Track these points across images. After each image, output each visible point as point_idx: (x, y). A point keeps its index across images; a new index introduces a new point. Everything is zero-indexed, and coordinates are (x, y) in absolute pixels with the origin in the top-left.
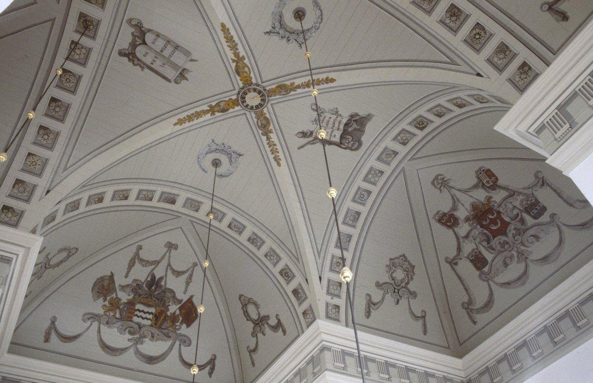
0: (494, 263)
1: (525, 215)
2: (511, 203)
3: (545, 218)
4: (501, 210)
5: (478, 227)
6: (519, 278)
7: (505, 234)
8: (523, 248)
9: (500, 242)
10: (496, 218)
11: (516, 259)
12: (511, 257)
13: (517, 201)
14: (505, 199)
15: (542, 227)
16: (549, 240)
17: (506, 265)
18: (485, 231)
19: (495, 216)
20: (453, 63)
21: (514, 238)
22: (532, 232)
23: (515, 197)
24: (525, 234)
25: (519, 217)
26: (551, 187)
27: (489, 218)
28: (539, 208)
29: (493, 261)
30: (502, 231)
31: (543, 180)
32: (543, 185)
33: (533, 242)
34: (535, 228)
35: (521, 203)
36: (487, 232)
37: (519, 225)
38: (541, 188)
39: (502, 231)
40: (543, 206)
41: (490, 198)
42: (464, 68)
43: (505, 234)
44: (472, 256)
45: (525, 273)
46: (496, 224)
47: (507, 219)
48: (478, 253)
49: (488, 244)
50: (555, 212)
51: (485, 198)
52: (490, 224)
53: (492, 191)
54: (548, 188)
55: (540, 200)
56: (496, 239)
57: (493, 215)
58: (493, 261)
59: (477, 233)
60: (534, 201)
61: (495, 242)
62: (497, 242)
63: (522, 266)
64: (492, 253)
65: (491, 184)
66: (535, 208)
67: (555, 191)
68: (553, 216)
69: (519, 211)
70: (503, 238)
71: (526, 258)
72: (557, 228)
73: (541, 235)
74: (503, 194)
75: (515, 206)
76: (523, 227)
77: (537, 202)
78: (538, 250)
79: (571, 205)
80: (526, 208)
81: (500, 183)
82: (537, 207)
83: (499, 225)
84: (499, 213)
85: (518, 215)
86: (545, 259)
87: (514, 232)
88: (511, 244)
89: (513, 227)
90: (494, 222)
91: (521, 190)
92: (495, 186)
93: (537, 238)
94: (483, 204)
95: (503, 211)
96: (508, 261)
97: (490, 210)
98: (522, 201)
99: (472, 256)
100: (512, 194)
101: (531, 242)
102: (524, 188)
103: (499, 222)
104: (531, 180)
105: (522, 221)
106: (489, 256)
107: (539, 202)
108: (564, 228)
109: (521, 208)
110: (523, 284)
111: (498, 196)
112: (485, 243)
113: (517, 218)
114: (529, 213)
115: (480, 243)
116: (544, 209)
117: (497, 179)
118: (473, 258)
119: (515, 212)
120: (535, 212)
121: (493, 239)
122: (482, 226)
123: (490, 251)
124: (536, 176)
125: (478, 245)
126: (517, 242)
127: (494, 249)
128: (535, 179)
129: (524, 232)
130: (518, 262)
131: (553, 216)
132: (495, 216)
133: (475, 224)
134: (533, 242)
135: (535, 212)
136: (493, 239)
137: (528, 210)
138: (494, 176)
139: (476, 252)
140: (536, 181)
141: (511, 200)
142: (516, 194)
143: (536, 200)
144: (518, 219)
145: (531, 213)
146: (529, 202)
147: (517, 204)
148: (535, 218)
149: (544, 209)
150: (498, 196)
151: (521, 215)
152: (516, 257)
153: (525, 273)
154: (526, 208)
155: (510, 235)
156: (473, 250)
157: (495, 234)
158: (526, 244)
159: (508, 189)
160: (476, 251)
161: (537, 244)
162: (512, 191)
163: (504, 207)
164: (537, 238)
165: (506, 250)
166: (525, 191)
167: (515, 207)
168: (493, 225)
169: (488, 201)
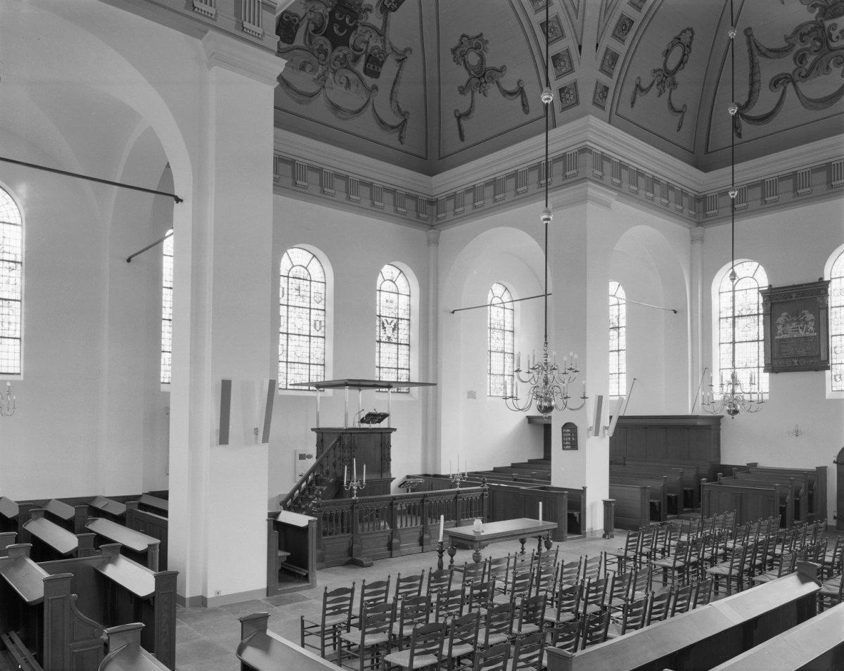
0: (296, 51)
1: (363, 58)
2: (371, 36)
3: (370, 81)
4: (360, 28)
5: (329, 9)
6: (300, 93)
7: (334, 48)
8: (331, 76)
9: (322, 45)
10: (348, 27)
11: (316, 76)
12: (313, 70)
13: (375, 43)
14: (374, 28)
15: (360, 85)
16: (352, 99)
17: (302, 68)
18: (327, 21)
19: (351, 25)
20: (607, 9)
21: (336, 60)
22: (351, 76)
23: (379, 38)
24: (346, 70)
25: (360, 53)
26: (399, 70)
27: (345, 19)
28: (376, 70)
29: (297, 48)
30: (337, 42)
31: (403, 59)
32: (399, 61)
33: (342, 83)
34: (355, 76)
35: (373, 48)
36: (327, 23)
37: (350, 58)
38: (396, 60)
39: (337, 42)
40: (380, 73)
41: (370, 10)
42: (602, 25)
43: (334, 48)
44: (287, 17)
45: (312, 96)
46: (341, 30)
47: (351, 41)
48: (296, 24)
49: (313, 31)
50: (379, 87)
51: (369, 5)
52: (338, 22)
53: (379, 8)
54: (397, 68)
55: (385, 66)
56: (323, 38)
57: (351, 22)
58: (297, 48)
59: (321, 11)
60: (381, 60)
61: (320, 40)
62: (320, 42)
63: (313, 88)
64: (305, 39)
65: (388, 6)
66: (374, 65)
67: (397, 76)
68: (375, 88)
69: (365, 49)
70: (328, 47)
71: (324, 87)
72: (366, 99)
73: (353, 87)
74: (379, 24)
75: (368, 42)
76: (350, 63)
77: (381, 64)
78: (337, 93)
79: (391, 99)
80: (370, 55)
81: (393, 16)
82: (376, 67)
83: (341, 35)
84: (355, 27)
85: (361, 50)
86: (336, 108)
87: (341, 57)
88: (327, 60)
89: (346, 52)
90: (343, 27)
91: (388, 42)
92: (385, 10)
93: (348, 85)
94: (360, 4)
95: (358, 32)
96: (308, 68)
97: (355, 16)
98: (377, 47)
99: (287, 17)
100: (382, 34)
101: (341, 81)
102: (390, 43)
103: (345, 32)
104: (401, 47)
105: (356, 59)
106: (299, 40)
107: (381, 67)
108: (370, 108)
109: (368, 51)
110: (300, 102)
111: (374, 19)
112: (312, 27)
113: (358, 51)
114: (367, 61)
115: (309, 20)
116: (376, 75)
117: (395, 10)
118: (286, 20)
119: (363, 46)
120: (371, 68)
121: (322, 35)
122: (332, 14)
123: (307, 37)
124: (406, 50)
125: (306, 18)
126: (332, 65)
127: (311, 42)
128: (403, 49)
129: (346, 68)
130: (314, 80)
131: (375, 88)
132: (351, 25)
133: (331, 4)
134: (342, 83)
135: (371, 68)
136: (322, 35)
137: (369, 59)
138: (398, 6)
139: (295, 20)
140: (400, 53)
141: (374, 34)
142: (383, 38)
143: (383, 62)
144: (356, 53)
145: (368, 64)
146: (378, 56)
147: (372, 43)
148: (365, 71)
149: (376, 75)
150: (374, 19)
151: (362, 54)
152: (317, 74)
153: (312, 96)
154: (370, 55)
155: (336, 53)
156: (296, 15)
157: (329, 34)
158: (337, 77)
159: (386, 26)
160: (297, 19)
161: (343, 89)
162: (385, 31)
163: (364, 30)
164: (348, 85)
165: (318, 58)
166: (388, 46)
167: (368, 43)
168: (338, 27)
169: (365, 9)
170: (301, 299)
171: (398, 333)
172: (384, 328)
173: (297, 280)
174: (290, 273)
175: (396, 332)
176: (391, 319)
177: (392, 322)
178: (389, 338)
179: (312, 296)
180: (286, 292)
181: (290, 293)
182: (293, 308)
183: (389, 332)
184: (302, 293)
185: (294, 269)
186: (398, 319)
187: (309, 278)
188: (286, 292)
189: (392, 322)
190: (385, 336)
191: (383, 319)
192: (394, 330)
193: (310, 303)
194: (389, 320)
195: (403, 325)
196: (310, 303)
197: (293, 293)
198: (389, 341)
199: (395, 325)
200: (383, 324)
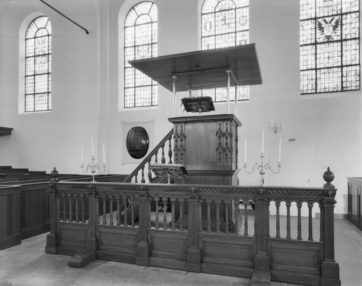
170: (227, 27)
171: (341, 29)
172: (321, 29)
173: (223, 13)
174: (217, 8)
175: (339, 28)
176: (331, 18)
177: (332, 20)
178: (328, 37)
179: (237, 20)
180: (213, 25)
181: (217, 24)
182: (220, 36)
183: (328, 31)
184: (227, 21)
185: (220, 4)
186: (342, 14)
187: (234, 7)
188: (213, 25)
189: (332, 20)
190: (323, 36)
191: (320, 20)
192: (335, 28)
193: (236, 27)
194: (327, 19)
195: (347, 20)
196: (236, 27)
197: (220, 23)
198: (329, 40)
199: (337, 23)
200: (320, 24)
